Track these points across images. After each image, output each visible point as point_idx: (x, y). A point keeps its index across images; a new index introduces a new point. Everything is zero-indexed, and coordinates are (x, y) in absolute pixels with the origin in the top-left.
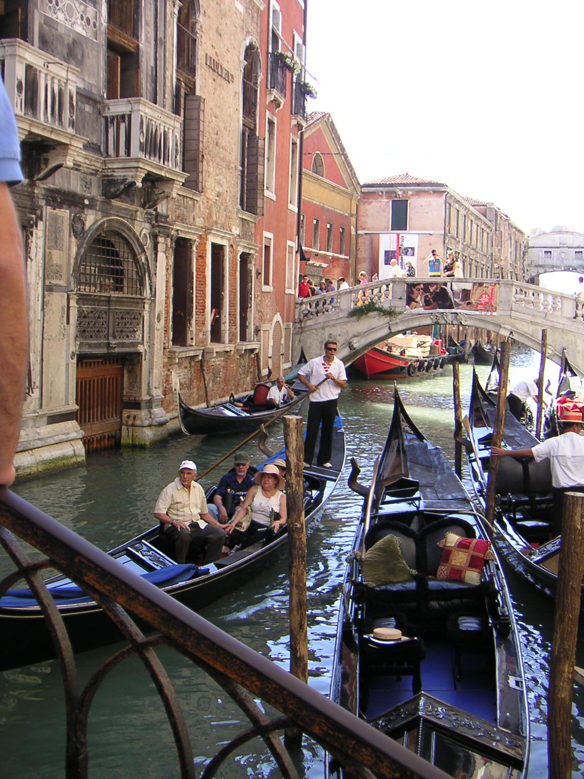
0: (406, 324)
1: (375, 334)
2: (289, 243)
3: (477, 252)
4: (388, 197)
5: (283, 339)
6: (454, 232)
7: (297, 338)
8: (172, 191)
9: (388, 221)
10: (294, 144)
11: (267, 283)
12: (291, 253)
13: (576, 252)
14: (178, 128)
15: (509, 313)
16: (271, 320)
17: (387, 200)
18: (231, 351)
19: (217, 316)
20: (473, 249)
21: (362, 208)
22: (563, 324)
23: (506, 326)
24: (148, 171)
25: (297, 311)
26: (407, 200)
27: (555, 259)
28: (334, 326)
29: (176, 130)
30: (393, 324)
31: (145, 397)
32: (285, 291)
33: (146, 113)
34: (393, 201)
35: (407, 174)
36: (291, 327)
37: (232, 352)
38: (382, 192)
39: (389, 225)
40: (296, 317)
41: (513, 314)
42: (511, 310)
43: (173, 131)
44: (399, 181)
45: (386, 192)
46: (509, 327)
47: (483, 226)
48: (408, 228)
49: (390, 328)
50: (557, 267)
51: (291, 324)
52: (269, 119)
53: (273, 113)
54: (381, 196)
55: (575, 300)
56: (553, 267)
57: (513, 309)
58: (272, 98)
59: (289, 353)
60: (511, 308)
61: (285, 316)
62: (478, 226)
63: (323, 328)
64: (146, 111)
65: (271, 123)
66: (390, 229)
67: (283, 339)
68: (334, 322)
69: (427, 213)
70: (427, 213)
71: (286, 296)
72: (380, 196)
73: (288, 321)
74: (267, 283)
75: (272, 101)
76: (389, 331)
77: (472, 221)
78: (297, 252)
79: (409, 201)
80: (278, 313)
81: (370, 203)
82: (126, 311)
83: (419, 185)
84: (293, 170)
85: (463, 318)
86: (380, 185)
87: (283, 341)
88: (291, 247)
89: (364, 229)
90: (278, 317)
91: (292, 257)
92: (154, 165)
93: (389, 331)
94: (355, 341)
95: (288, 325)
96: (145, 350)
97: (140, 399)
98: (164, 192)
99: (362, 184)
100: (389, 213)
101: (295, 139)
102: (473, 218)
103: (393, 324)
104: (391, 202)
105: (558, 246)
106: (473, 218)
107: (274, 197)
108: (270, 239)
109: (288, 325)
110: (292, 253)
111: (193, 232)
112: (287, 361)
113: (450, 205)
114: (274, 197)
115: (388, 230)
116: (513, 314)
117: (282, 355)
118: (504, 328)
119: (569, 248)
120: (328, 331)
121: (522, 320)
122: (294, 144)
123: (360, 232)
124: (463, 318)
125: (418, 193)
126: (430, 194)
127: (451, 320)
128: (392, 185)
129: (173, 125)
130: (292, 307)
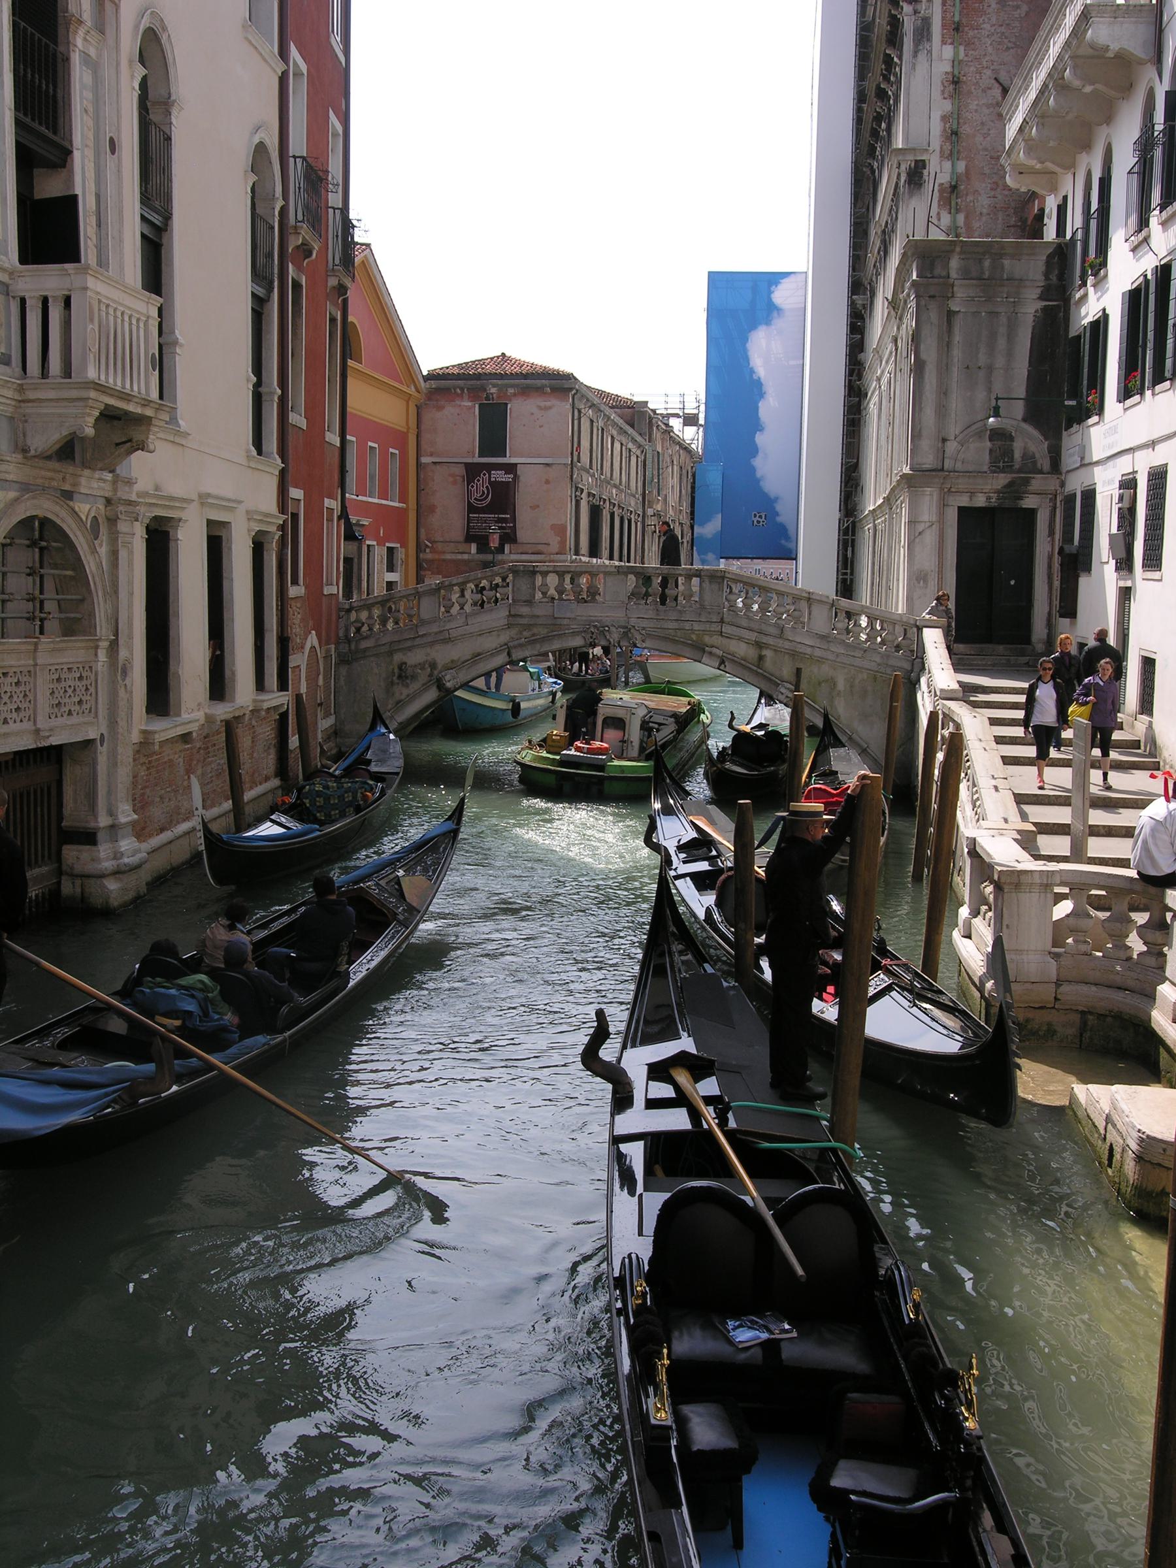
0: (538, 646)
1: (481, 665)
2: (327, 502)
3: (622, 491)
4: (474, 397)
5: (321, 677)
6: (585, 459)
7: (343, 670)
8: (147, 438)
9: (474, 440)
10: (333, 320)
11: (295, 582)
12: (330, 520)
14: (153, 318)
15: (715, 627)
16: (303, 648)
17: (470, 404)
18: (244, 714)
19: (218, 653)
20: (615, 486)
21: (429, 416)
23: (714, 650)
24: (106, 404)
25: (342, 623)
26: (506, 404)
28: (410, 649)
29: (151, 321)
30: (515, 647)
31: (103, 821)
32: (322, 591)
33: (98, 293)
34: (480, 405)
35: (503, 355)
36: (333, 653)
37: (247, 717)
38: (462, 389)
39: (474, 447)
40: (341, 634)
41: (727, 629)
42: (722, 621)
43: (146, 323)
44: (489, 369)
45: (468, 389)
47: (630, 445)
48: (508, 455)
49: (509, 654)
51: (333, 646)
52: (293, 279)
53: (299, 268)
54: (461, 396)
55: (833, 605)
57: (725, 620)
58: (300, 241)
59: (330, 699)
60: (722, 619)
61: (324, 633)
62: (622, 444)
63: (391, 653)
64: (99, 290)
65: (297, 286)
66: (477, 455)
67: (321, 677)
68: (409, 644)
69: (541, 427)
70: (541, 427)
71: (324, 598)
72: (458, 395)
73: (328, 643)
74: (295, 582)
75: (298, 247)
76: (507, 659)
77: (612, 437)
78: (339, 518)
79: (509, 406)
80: (314, 632)
81: (440, 408)
82: (66, 667)
83: (526, 376)
84: (330, 370)
85: (638, 637)
86: (458, 377)
87: (321, 682)
88: (331, 510)
89: (431, 455)
90: (313, 640)
91: (333, 527)
92: (117, 394)
93: (507, 659)
94: (447, 678)
95: (328, 651)
96: (102, 734)
97: (92, 825)
98: (130, 441)
99: (425, 373)
100: (474, 426)
101: (334, 313)
102: (615, 433)
103: (515, 647)
104: (477, 406)
106: (615, 433)
107: (303, 424)
108: (299, 500)
109: (328, 651)
110: (332, 520)
111: (177, 505)
112: (327, 715)
113: (580, 412)
114: (303, 424)
115: (474, 457)
116: (727, 629)
117: (320, 705)
118: (710, 653)
120: (398, 658)
122: (333, 320)
123: (424, 460)
124: (638, 637)
125: (525, 392)
127: (617, 639)
128: (478, 377)
129: (145, 312)
130: (334, 618)
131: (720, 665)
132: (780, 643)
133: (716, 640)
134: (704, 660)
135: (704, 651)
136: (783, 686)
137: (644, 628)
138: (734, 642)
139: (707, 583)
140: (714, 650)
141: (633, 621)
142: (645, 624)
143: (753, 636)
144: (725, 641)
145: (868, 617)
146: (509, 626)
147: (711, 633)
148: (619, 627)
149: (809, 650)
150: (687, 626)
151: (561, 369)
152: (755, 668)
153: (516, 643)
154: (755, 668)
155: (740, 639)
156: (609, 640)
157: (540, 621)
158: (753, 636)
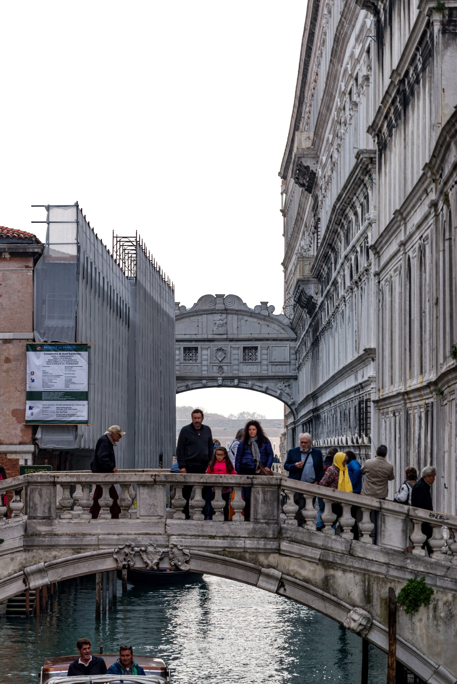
0: (60, 570)
13: (245, 348)
15: (272, 545)
22: (387, 564)
23: (272, 571)
27: (204, 363)
41: (285, 545)
46: (277, 573)
49: (24, 582)
50: (214, 379)
56: (200, 379)
105: (210, 337)
116: (285, 545)
119: (231, 340)
121: (301, 557)
126: (5, 259)
131: (279, 588)
132: (350, 562)
133: (273, 559)
134: (260, 583)
135: (260, 573)
136: (355, 612)
137: (187, 547)
138: (294, 561)
139: (260, 492)
140: (272, 571)
141: (174, 540)
142: (188, 542)
143: (317, 554)
144: (284, 559)
145: (450, 529)
146: (27, 548)
147: (267, 552)
148: (158, 546)
149: (383, 570)
150: (240, 543)
151: (10, 227)
152: (320, 591)
153: (34, 568)
154: (320, 591)
155: (301, 557)
156: (146, 563)
157: (63, 540)
158: (317, 554)
